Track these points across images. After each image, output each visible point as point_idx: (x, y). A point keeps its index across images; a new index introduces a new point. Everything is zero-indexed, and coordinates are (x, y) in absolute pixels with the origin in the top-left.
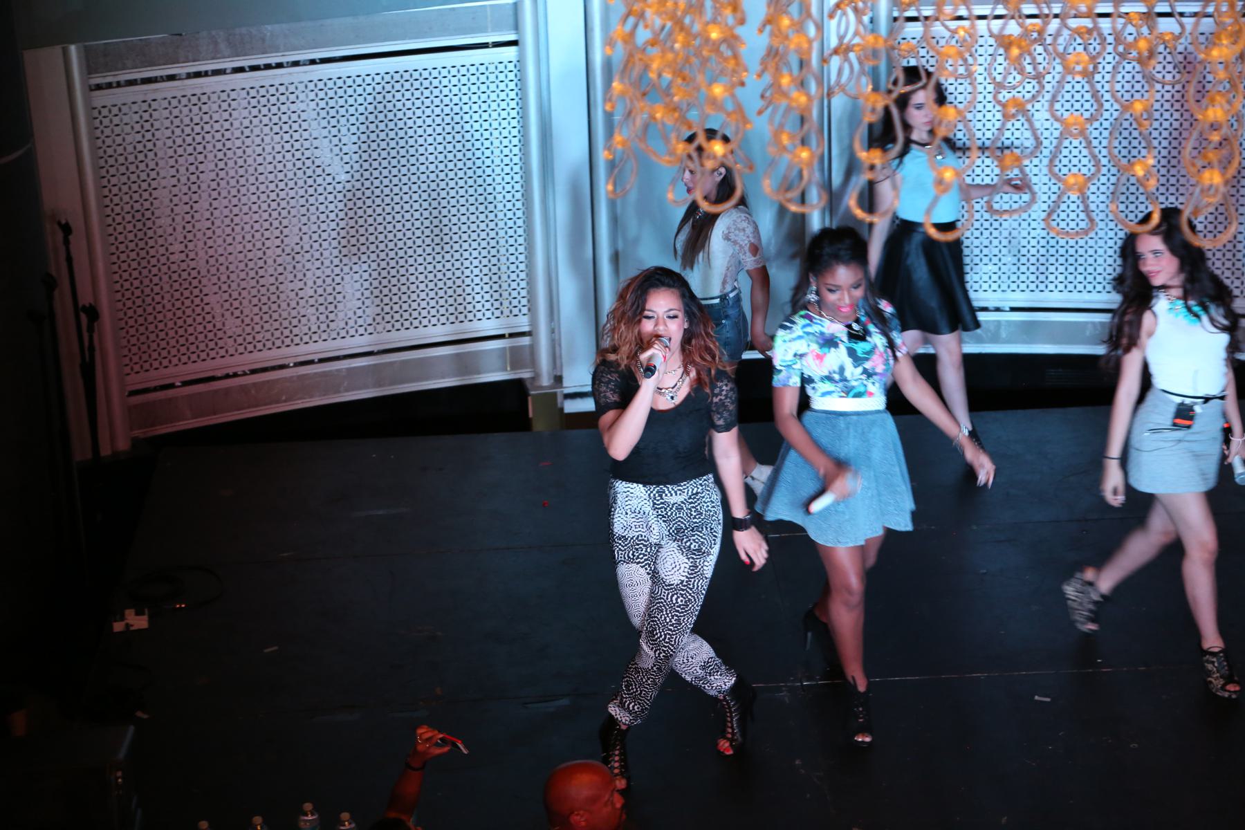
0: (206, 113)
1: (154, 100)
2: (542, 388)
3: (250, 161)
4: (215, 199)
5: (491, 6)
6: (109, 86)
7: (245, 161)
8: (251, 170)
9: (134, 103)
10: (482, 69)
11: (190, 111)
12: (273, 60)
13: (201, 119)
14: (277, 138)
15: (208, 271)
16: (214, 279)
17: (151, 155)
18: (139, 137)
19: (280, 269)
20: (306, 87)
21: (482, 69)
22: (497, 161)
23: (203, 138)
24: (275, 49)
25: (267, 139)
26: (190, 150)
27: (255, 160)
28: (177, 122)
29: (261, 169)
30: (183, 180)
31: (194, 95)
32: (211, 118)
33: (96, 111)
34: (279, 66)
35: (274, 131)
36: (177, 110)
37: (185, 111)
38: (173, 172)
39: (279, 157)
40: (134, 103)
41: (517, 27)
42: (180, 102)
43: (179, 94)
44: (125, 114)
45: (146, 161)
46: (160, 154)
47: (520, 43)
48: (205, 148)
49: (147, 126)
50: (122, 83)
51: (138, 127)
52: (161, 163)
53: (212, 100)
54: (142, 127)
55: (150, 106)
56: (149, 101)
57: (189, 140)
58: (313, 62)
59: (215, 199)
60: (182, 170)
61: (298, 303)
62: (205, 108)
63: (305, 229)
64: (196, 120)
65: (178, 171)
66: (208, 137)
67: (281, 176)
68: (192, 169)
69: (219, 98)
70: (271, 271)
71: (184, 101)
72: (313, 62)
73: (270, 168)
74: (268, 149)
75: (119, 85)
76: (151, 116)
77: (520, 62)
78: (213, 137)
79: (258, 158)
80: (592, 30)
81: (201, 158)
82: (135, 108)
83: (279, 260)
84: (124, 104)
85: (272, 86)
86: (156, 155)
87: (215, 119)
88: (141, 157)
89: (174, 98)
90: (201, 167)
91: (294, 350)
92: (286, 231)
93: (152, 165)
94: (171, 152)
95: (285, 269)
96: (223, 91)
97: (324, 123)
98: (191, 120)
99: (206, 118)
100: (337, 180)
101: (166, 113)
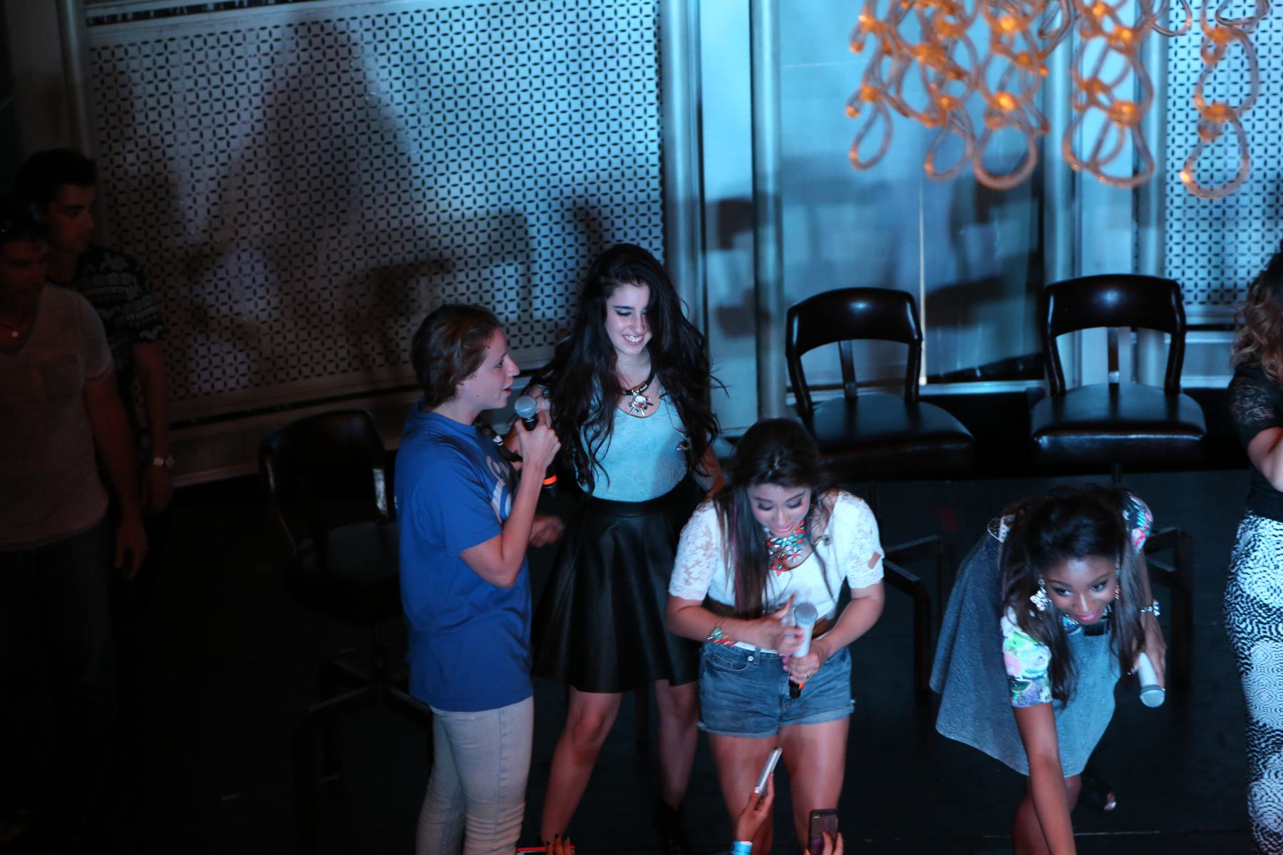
0: (240, 58)
1: (172, 39)
3: (297, 122)
4: (251, 173)
6: (113, 19)
7: (291, 123)
8: (298, 135)
9: (145, 43)
11: (220, 54)
13: (234, 65)
15: (240, 270)
16: (248, 281)
17: (166, 113)
18: (151, 89)
23: (236, 91)
26: (218, 107)
27: (304, 122)
28: (201, 69)
29: (312, 133)
30: (209, 147)
31: (224, 33)
32: (247, 63)
33: (95, 54)
36: (202, 53)
37: (213, 54)
38: (195, 135)
40: (145, 43)
42: (205, 42)
43: (204, 32)
44: (133, 58)
45: (160, 121)
46: (179, 112)
48: (238, 104)
49: (162, 74)
50: (130, 16)
51: (149, 75)
52: (180, 124)
53: (248, 39)
54: (156, 75)
55: (166, 47)
56: (165, 40)
57: (217, 93)
59: (251, 173)
60: (208, 134)
62: (238, 51)
64: (227, 66)
65: (201, 135)
66: (242, 90)
68: (221, 132)
69: (258, 37)
71: (212, 41)
75: (125, 18)
76: (167, 60)
78: (249, 90)
81: (232, 117)
82: (146, 50)
84: (133, 45)
86: (173, 113)
87: (251, 66)
88: (153, 115)
89: (198, 36)
90: (233, 130)
92: (343, 218)
93: (168, 127)
94: (192, 110)
96: (263, 28)
98: (221, 66)
99: (240, 64)
101: (187, 57)
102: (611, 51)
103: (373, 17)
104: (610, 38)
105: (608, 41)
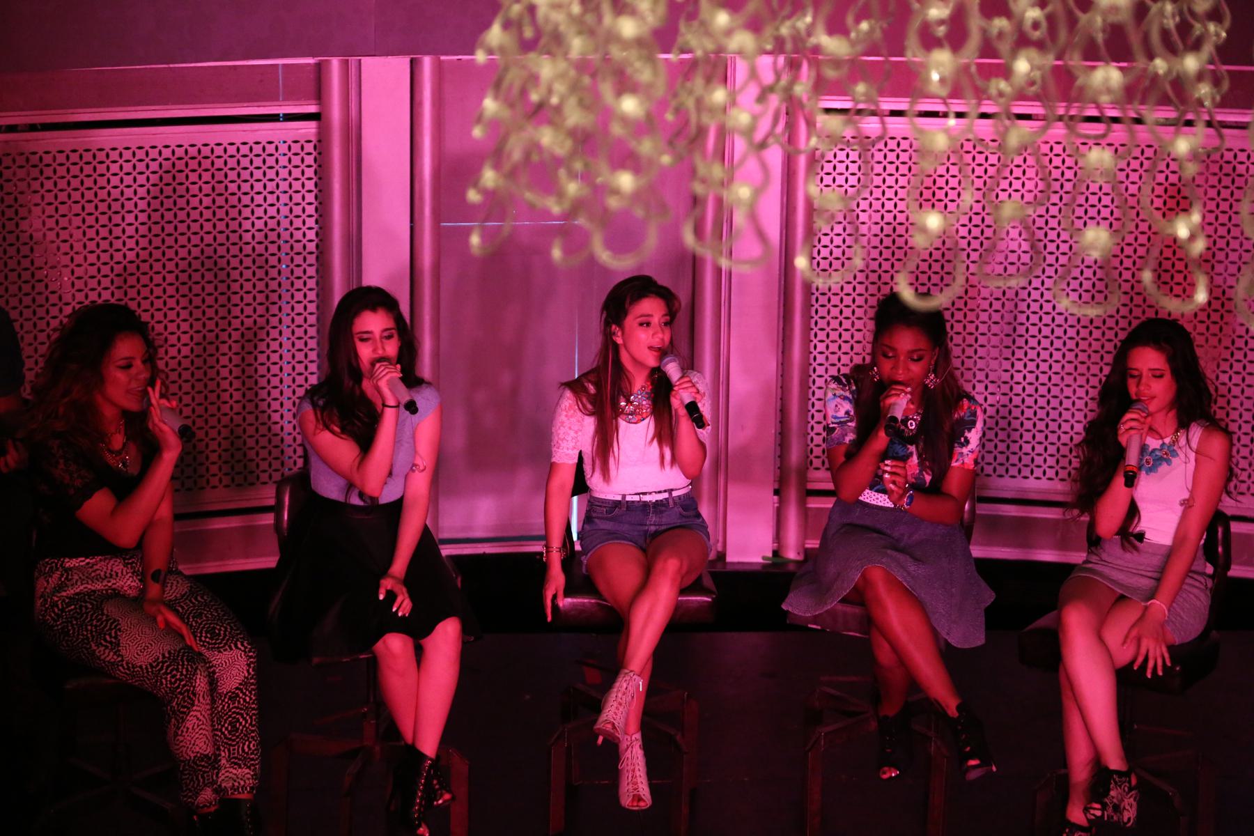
5: (284, 65)
10: (270, 149)
21: (270, 149)
41: (319, 92)
58: (33, 128)
72: (33, 128)
77: (322, 144)
80: (421, 103)
102: (271, 199)
105: (269, 189)
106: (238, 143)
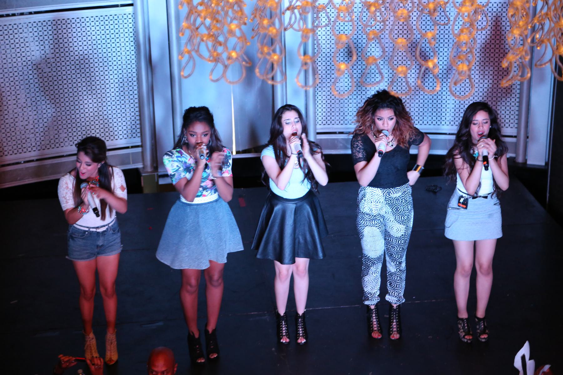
2: (148, 172)
10: (116, 17)
12: (10, 12)
14: (13, 51)
19: (16, 115)
20: (28, 25)
21: (116, 17)
22: (124, 62)
24: (11, 7)
25: (8, 51)
34: (14, 15)
35: (12, 47)
39: (14, 60)
47: (134, 5)
58: (30, 13)
61: (25, 132)
63: (28, 95)
67: (15, 69)
70: (11, 116)
72: (30, 13)
73: (10, 65)
74: (9, 56)
77: (135, 14)
79: (3, 60)
83: (15, 111)
85: (10, 25)
91: (23, 155)
92: (19, 97)
95: (18, 115)
97: (37, 43)
100: (44, 71)
103: (27, 23)
104: (117, 31)
106: (104, 16)
